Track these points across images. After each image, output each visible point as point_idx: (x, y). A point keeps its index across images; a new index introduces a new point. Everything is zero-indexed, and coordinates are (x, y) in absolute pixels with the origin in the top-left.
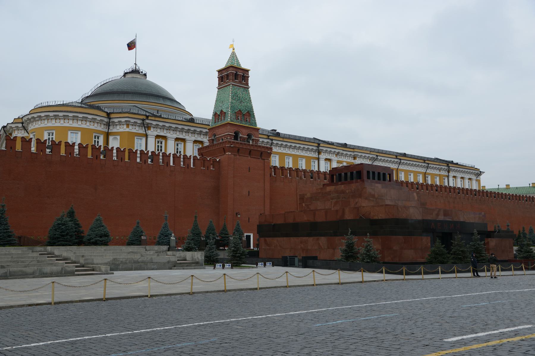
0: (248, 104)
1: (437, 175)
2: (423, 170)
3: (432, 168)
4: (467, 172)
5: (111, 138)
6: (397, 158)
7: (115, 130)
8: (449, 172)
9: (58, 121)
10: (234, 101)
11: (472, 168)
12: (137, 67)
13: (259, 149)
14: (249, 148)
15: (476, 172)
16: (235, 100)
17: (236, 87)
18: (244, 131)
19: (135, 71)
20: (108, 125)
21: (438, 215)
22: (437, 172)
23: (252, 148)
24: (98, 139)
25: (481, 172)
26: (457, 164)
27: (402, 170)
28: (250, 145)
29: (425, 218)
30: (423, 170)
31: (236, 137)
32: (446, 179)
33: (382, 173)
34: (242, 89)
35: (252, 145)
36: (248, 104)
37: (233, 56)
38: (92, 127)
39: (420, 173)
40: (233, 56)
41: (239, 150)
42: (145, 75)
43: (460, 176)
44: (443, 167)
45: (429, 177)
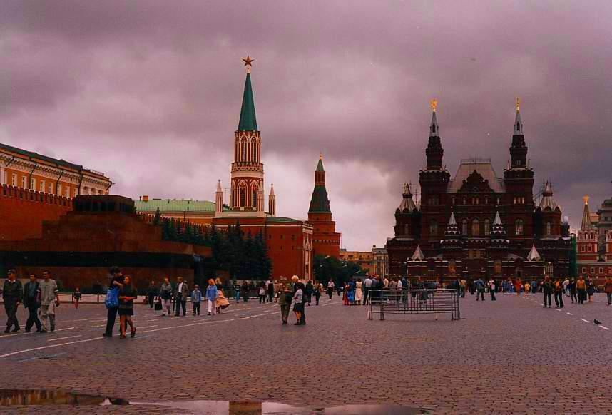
1: (68, 184)
2: (55, 178)
3: (67, 176)
4: (99, 183)
6: (31, 161)
8: (80, 182)
11: (101, 176)
15: (108, 183)
22: (69, 182)
25: (111, 183)
26: (88, 171)
27: (35, 176)
30: (55, 178)
32: (77, 189)
39: (52, 180)
43: (91, 187)
44: (76, 175)
45: (15, 178)
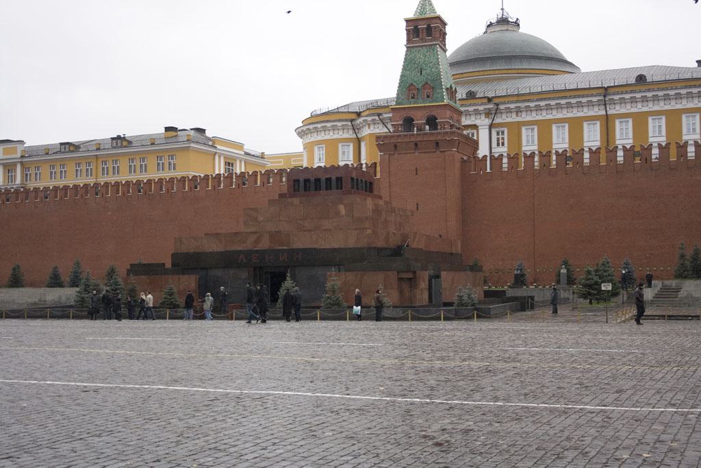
0: (433, 70)
5: (363, 144)
7: (363, 135)
9: (336, 132)
10: (408, 72)
12: (505, 14)
14: (413, 139)
16: (409, 70)
17: (413, 50)
19: (503, 21)
20: (355, 129)
21: (257, 241)
23: (419, 139)
24: (232, 166)
28: (413, 135)
29: (228, 249)
31: (409, 122)
33: (323, 180)
34: (425, 49)
36: (433, 70)
38: (336, 136)
41: (396, 146)
42: (517, 24)
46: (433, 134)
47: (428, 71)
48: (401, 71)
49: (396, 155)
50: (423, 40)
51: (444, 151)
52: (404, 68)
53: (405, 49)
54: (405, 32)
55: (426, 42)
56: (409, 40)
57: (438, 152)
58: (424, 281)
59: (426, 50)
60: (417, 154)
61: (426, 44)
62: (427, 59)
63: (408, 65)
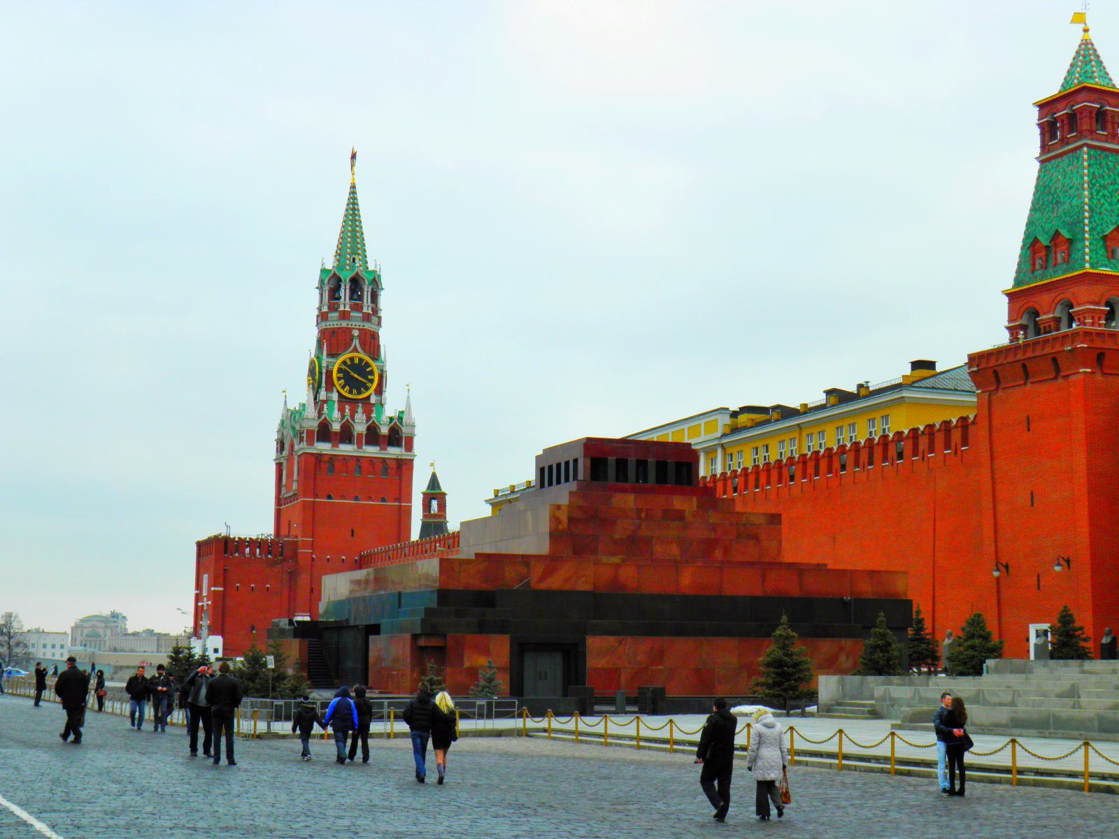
13: (1048, 350)
18: (1046, 298)
34: (1066, 159)
35: (1026, 345)
37: (1087, 54)
40: (1087, 54)
46: (1046, 341)
47: (1067, 205)
48: (1027, 212)
49: (1000, 393)
50: (1064, 141)
51: (1068, 375)
52: (1034, 208)
53: (1037, 165)
54: (1037, 131)
55: (1068, 144)
56: (1044, 148)
57: (1060, 380)
58: (487, 653)
59: (1067, 161)
60: (1029, 386)
61: (1066, 148)
62: (1067, 181)
63: (1039, 199)
